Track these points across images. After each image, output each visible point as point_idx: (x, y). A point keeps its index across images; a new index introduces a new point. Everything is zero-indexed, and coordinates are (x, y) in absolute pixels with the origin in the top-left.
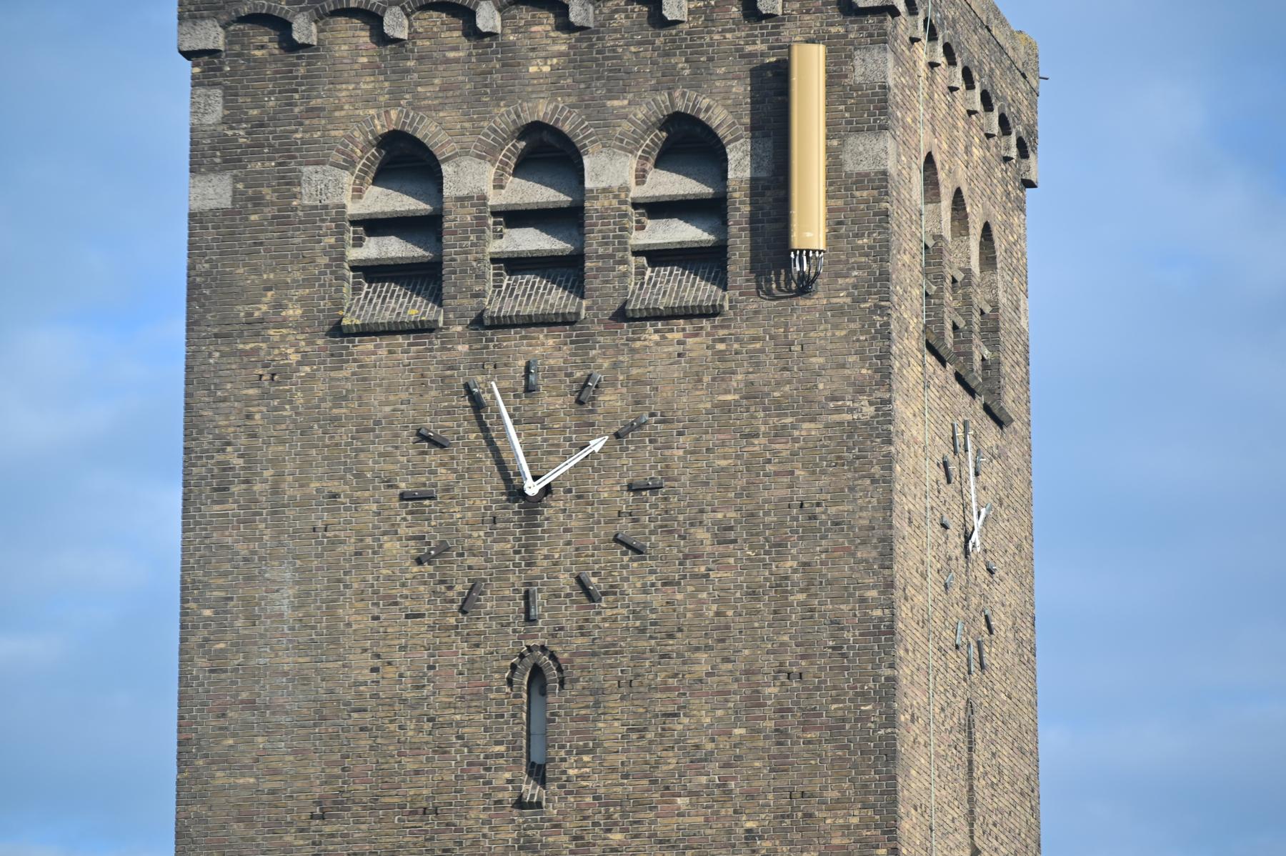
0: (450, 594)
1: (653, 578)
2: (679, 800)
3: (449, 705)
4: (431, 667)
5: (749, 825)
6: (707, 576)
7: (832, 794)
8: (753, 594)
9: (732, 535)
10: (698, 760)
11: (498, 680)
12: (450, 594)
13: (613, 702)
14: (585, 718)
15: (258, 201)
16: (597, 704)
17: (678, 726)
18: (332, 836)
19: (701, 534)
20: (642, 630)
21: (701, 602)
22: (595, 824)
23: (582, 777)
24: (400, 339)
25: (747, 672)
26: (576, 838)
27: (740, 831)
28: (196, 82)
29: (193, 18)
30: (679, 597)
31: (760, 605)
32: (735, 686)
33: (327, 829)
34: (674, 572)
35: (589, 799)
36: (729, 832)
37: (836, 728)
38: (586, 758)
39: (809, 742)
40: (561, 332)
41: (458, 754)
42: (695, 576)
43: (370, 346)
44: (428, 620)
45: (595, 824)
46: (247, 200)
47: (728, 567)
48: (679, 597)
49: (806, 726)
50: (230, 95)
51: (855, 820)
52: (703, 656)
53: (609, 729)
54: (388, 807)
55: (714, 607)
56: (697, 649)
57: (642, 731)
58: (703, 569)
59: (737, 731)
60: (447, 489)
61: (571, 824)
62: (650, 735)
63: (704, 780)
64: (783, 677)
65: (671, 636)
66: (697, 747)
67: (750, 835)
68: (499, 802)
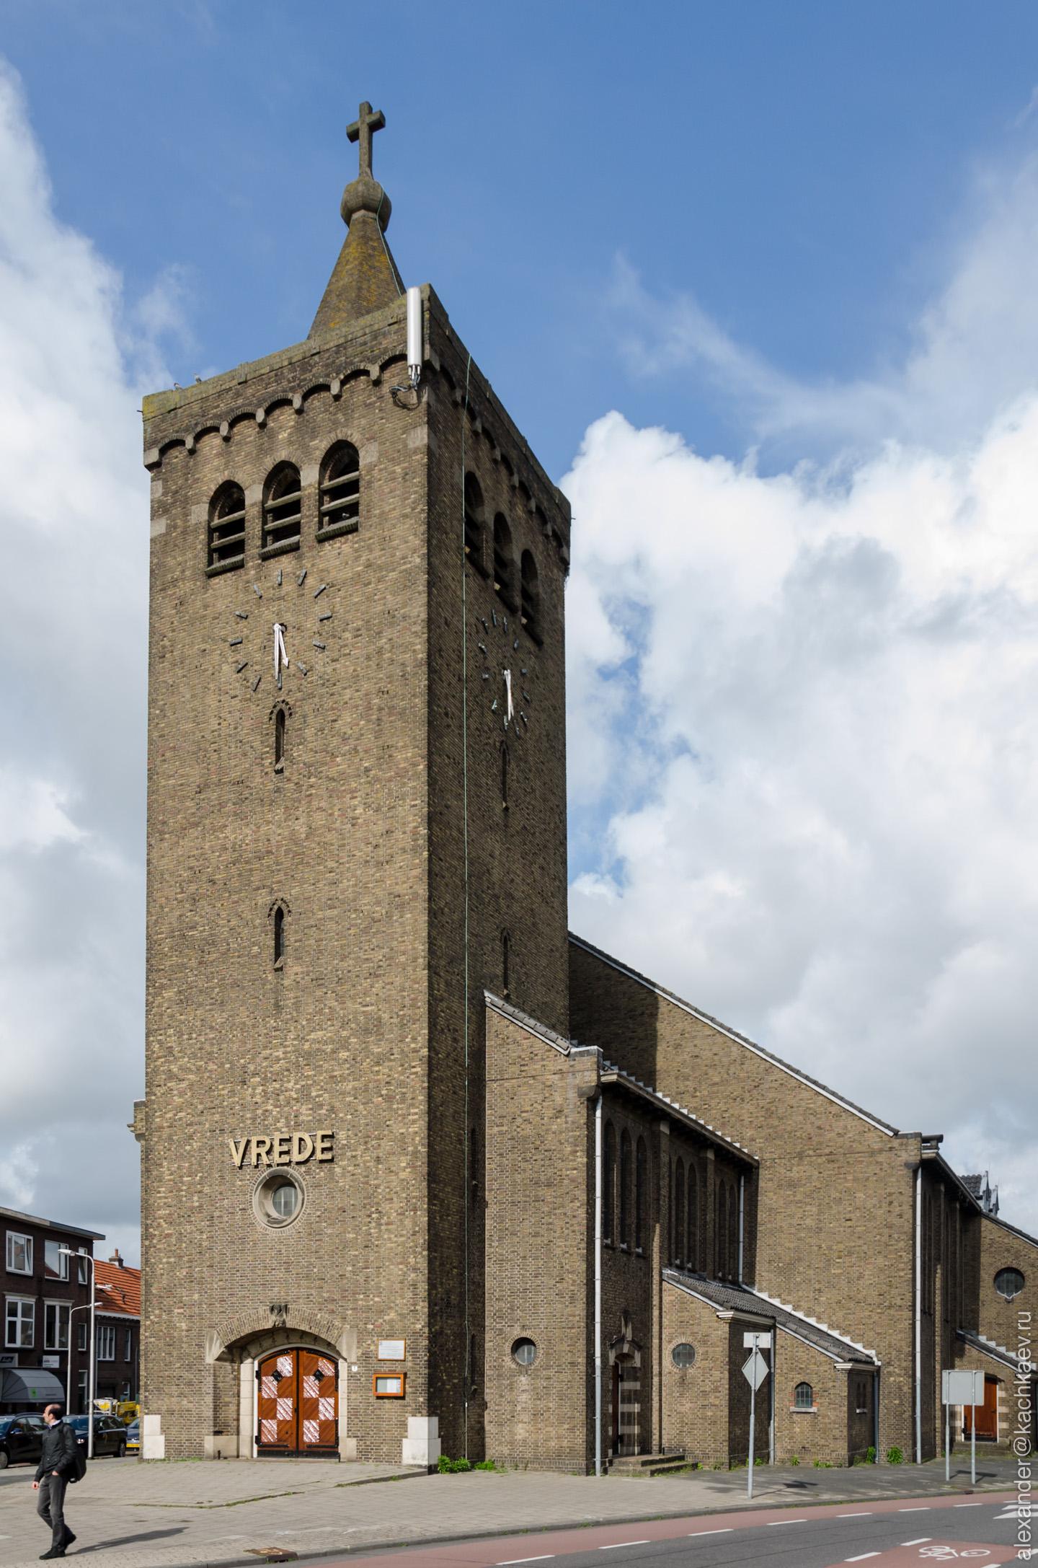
0: (249, 684)
1: (328, 659)
2: (338, 759)
3: (247, 734)
4: (241, 718)
5: (366, 765)
6: (350, 654)
7: (401, 744)
8: (368, 658)
9: (359, 633)
10: (345, 739)
11: (266, 719)
12: (249, 684)
13: (310, 720)
14: (300, 729)
15: (175, 527)
16: (305, 721)
17: (337, 725)
18: (204, 800)
19: (348, 635)
20: (323, 685)
21: (347, 666)
22: (304, 776)
23: (299, 756)
24: (229, 574)
25: (367, 695)
26: (296, 784)
27: (362, 768)
28: (153, 480)
29: (149, 449)
30: (338, 666)
31: (371, 663)
32: (361, 702)
33: (202, 797)
34: (336, 655)
35: (302, 765)
36: (358, 769)
37: (402, 713)
38: (300, 747)
39: (391, 722)
40: (291, 555)
41: (252, 755)
42: (345, 655)
43: (217, 581)
44: (239, 698)
45: (304, 776)
46: (172, 527)
47: (358, 648)
48: (338, 666)
49: (390, 714)
50: (165, 481)
51: (409, 755)
52: (348, 691)
53: (309, 732)
54: (225, 783)
55: (352, 668)
56: (345, 688)
57: (322, 730)
58: (348, 651)
59: (362, 722)
60: (247, 637)
61: (295, 778)
62: (326, 732)
63: (347, 748)
64: (381, 694)
65: (335, 685)
66: (345, 733)
67: (367, 770)
68: (266, 773)
